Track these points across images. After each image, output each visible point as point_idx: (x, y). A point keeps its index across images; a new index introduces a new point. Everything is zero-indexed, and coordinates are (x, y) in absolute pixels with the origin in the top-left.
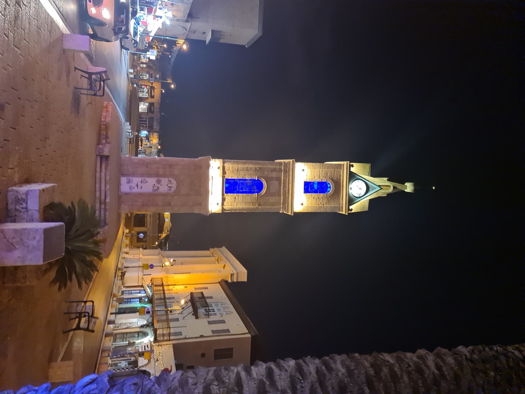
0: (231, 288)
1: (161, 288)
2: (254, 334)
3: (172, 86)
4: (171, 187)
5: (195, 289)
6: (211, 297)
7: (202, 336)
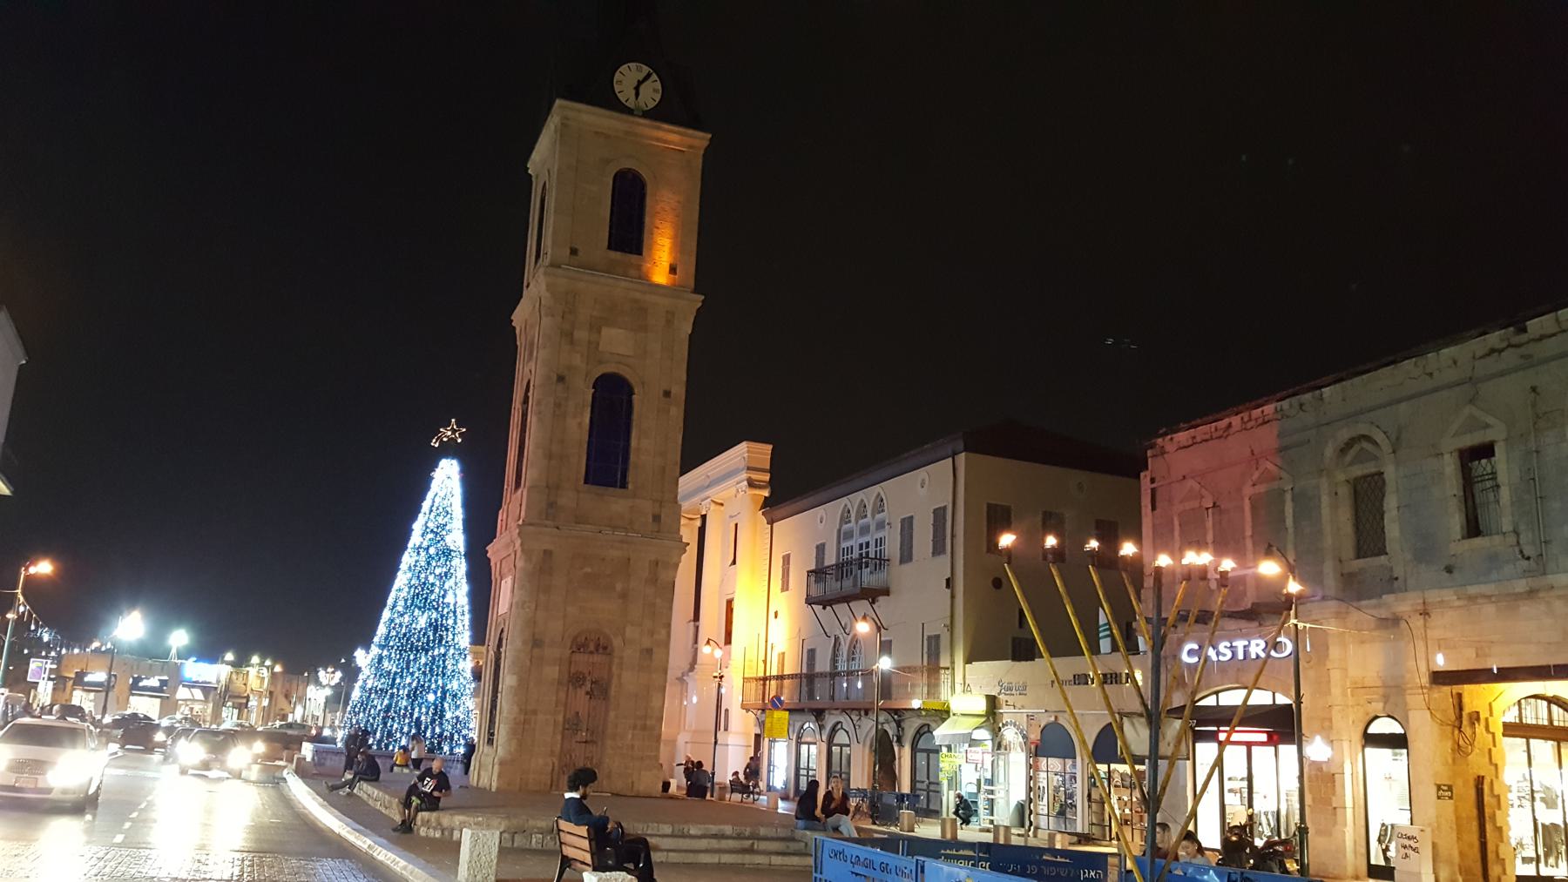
2: (961, 445)
4: (597, 647)
6: (821, 549)
7: (949, 583)
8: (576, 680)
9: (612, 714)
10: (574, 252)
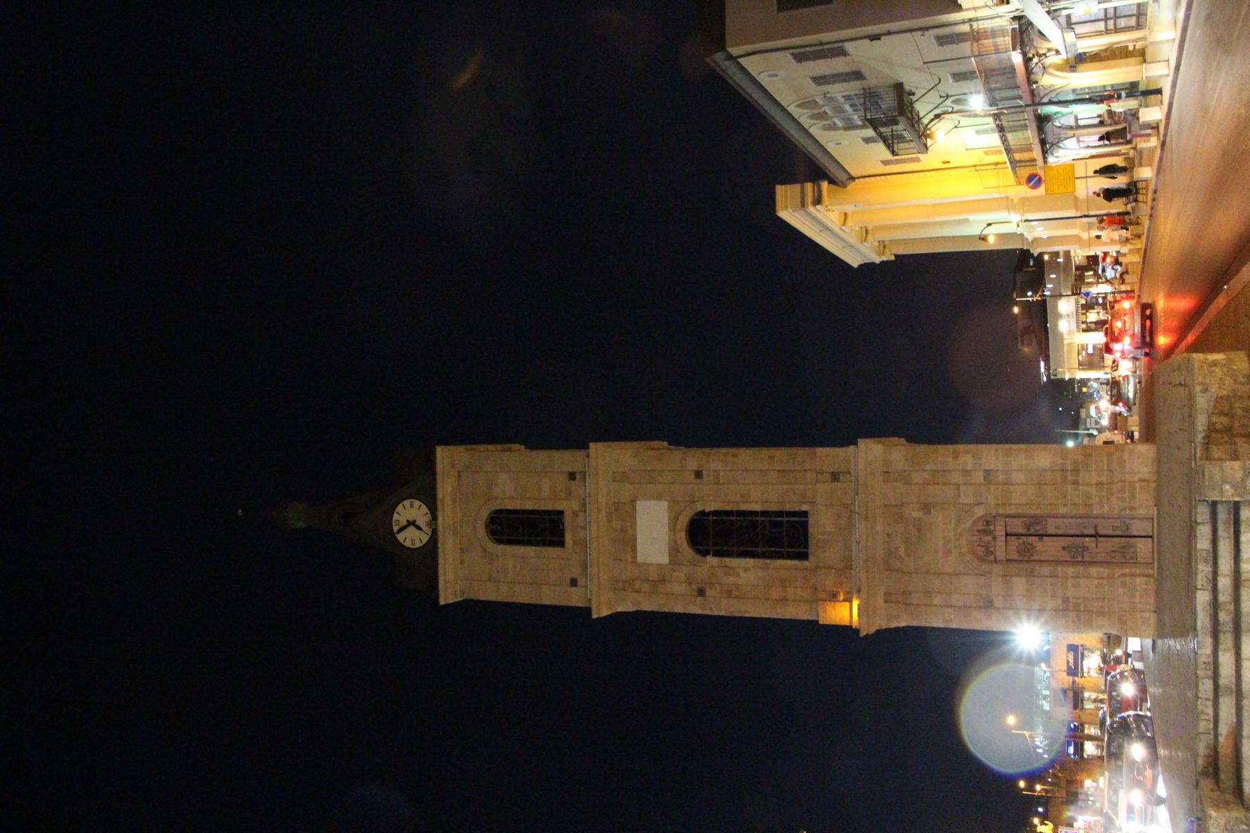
0: (817, 172)
1: (1017, 156)
2: (719, 56)
3: (1011, 720)
4: (986, 532)
5: (918, 160)
6: (867, 140)
7: (874, 38)
9: (1062, 510)
10: (574, 582)
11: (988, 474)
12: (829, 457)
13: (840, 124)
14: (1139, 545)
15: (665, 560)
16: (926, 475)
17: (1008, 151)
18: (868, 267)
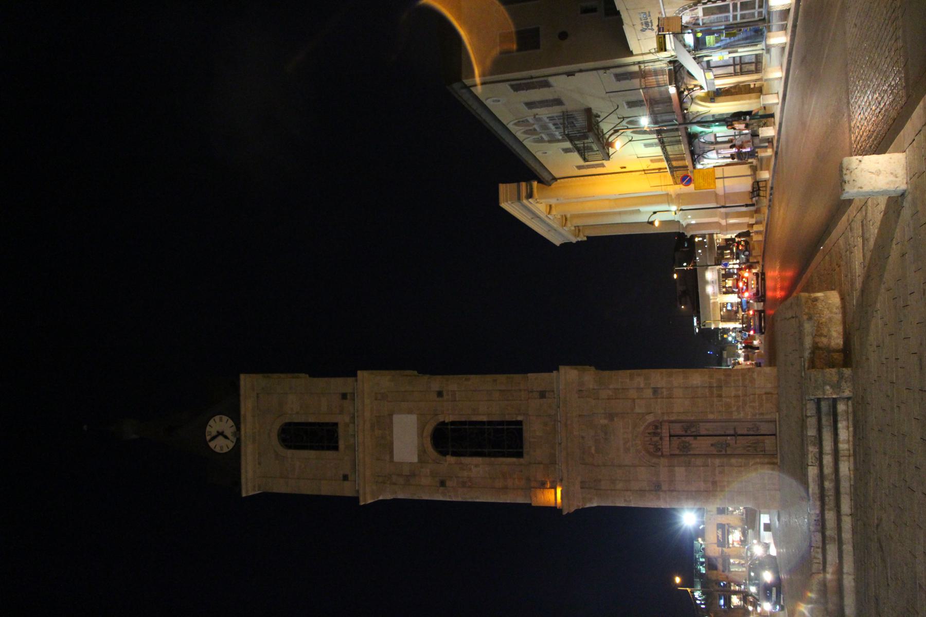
0: (527, 173)
1: (675, 164)
2: (456, 86)
3: (678, 580)
4: (655, 434)
6: (566, 151)
7: (570, 74)
8: (685, 449)
9: (711, 417)
10: (345, 478)
11: (655, 391)
12: (537, 380)
13: (545, 138)
14: (767, 441)
15: (415, 460)
16: (610, 393)
17: (668, 160)
18: (567, 246)
